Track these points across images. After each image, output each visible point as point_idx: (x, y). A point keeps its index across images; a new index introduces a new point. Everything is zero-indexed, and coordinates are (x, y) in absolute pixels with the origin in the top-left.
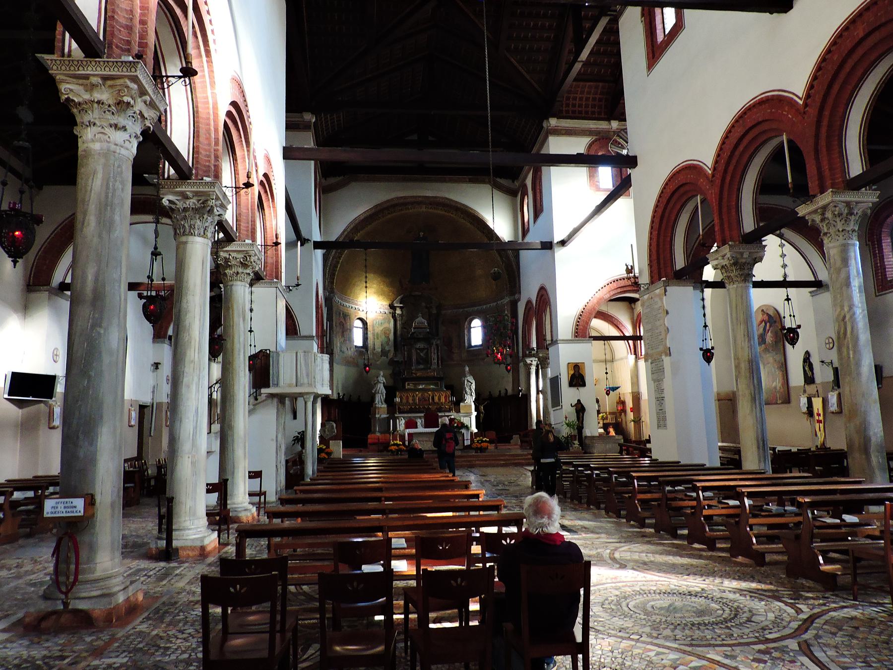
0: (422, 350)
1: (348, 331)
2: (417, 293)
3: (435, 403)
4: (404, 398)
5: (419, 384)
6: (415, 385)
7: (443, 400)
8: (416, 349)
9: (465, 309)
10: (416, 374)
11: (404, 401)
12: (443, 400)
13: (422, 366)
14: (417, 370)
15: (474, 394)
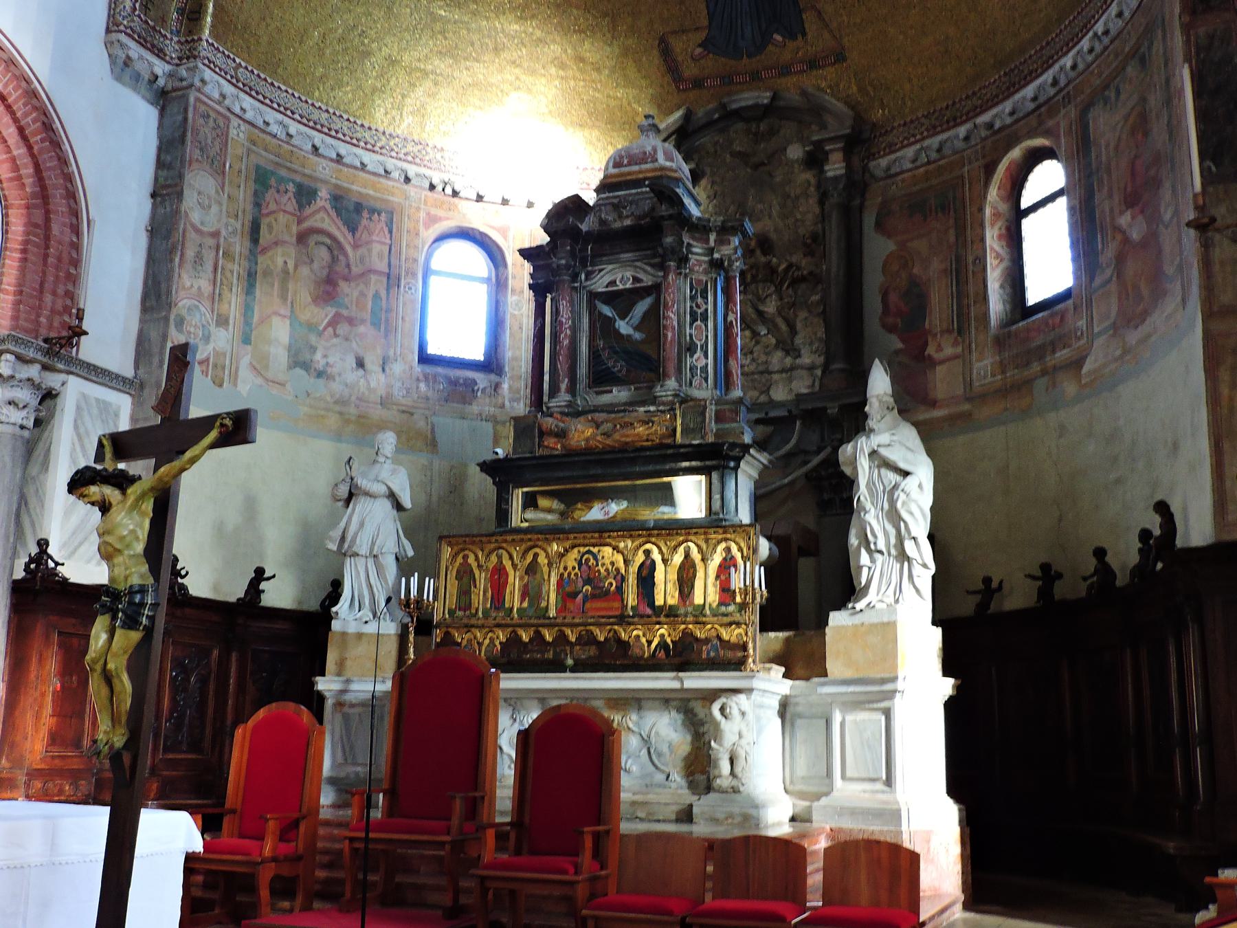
0: (622, 300)
1: (376, 284)
2: (748, 98)
3: (658, 611)
4: (482, 579)
5: (589, 497)
6: (572, 499)
7: (705, 591)
8: (593, 296)
9: (982, 119)
10: (561, 434)
11: (480, 597)
12: (705, 591)
13: (619, 394)
14: (574, 413)
15: (921, 553)
